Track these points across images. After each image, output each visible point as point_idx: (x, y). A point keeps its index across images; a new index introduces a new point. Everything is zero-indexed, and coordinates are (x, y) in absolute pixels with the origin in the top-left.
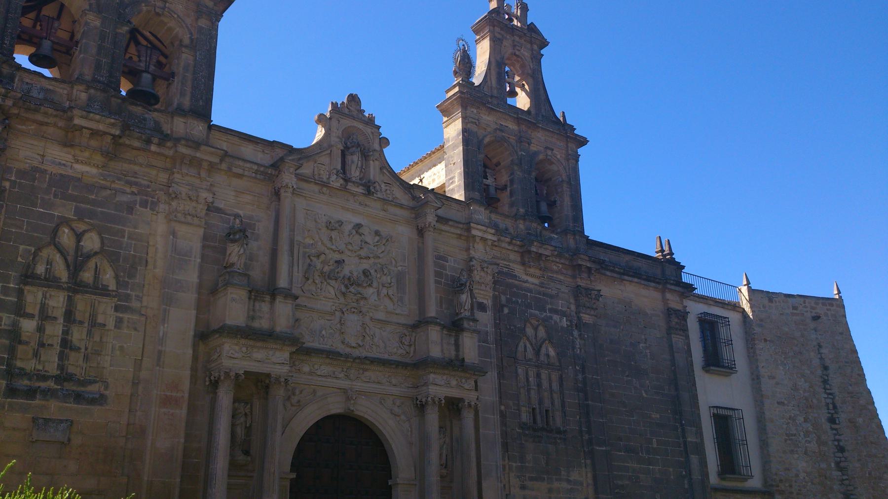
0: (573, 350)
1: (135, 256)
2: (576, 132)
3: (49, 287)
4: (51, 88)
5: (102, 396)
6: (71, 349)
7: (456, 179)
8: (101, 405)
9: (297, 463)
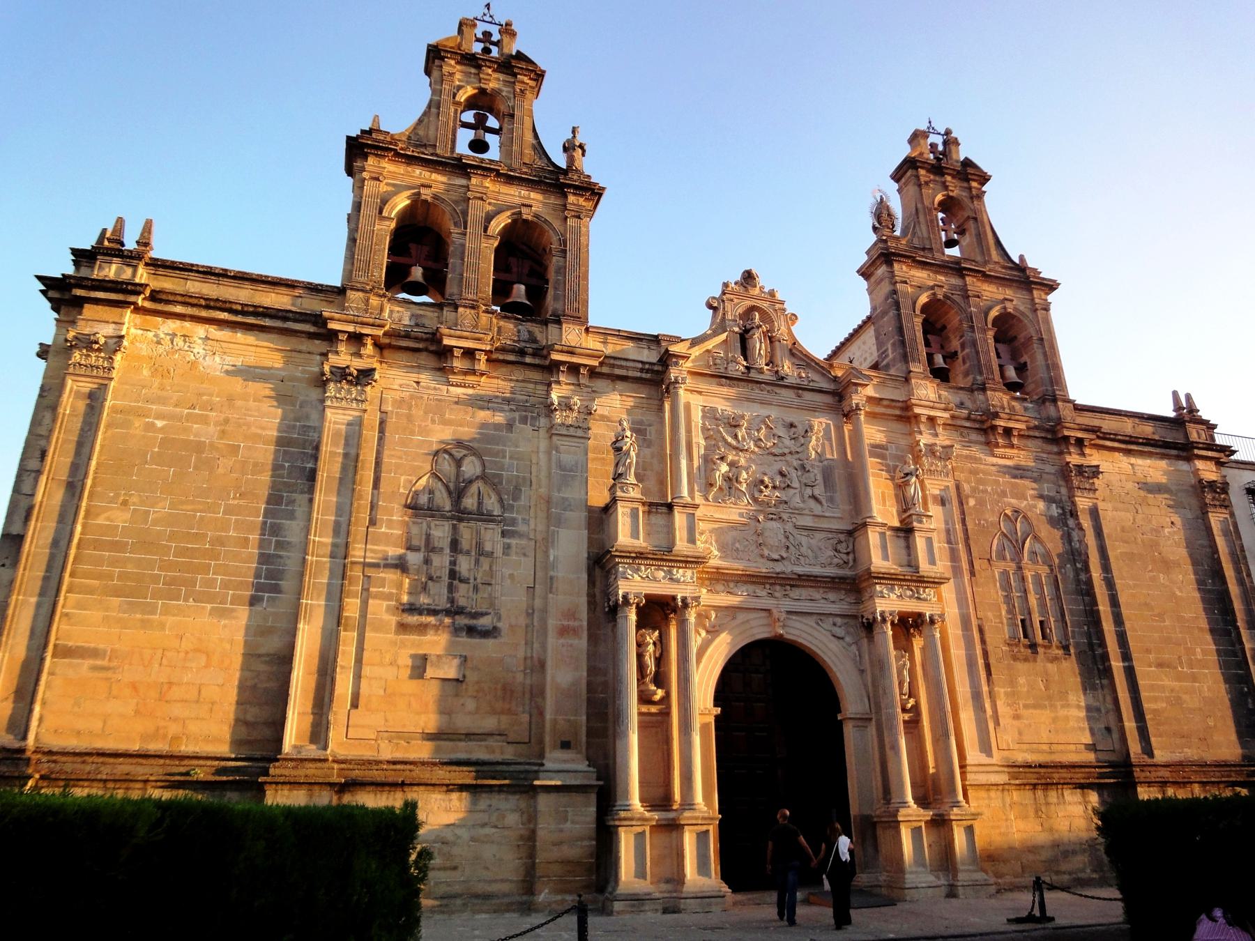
0: (1071, 545)
1: (518, 477)
2: (1041, 275)
3: (432, 516)
4: (421, 312)
5: (495, 628)
6: (461, 581)
7: (890, 351)
8: (495, 637)
9: (720, 697)
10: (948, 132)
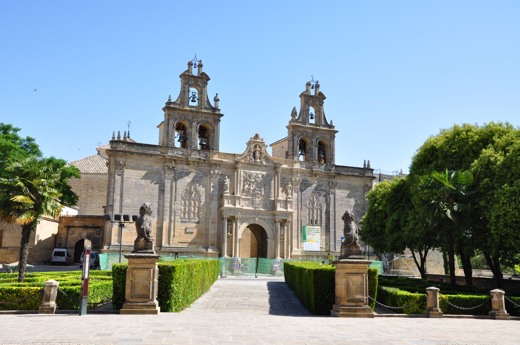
10: (317, 82)
